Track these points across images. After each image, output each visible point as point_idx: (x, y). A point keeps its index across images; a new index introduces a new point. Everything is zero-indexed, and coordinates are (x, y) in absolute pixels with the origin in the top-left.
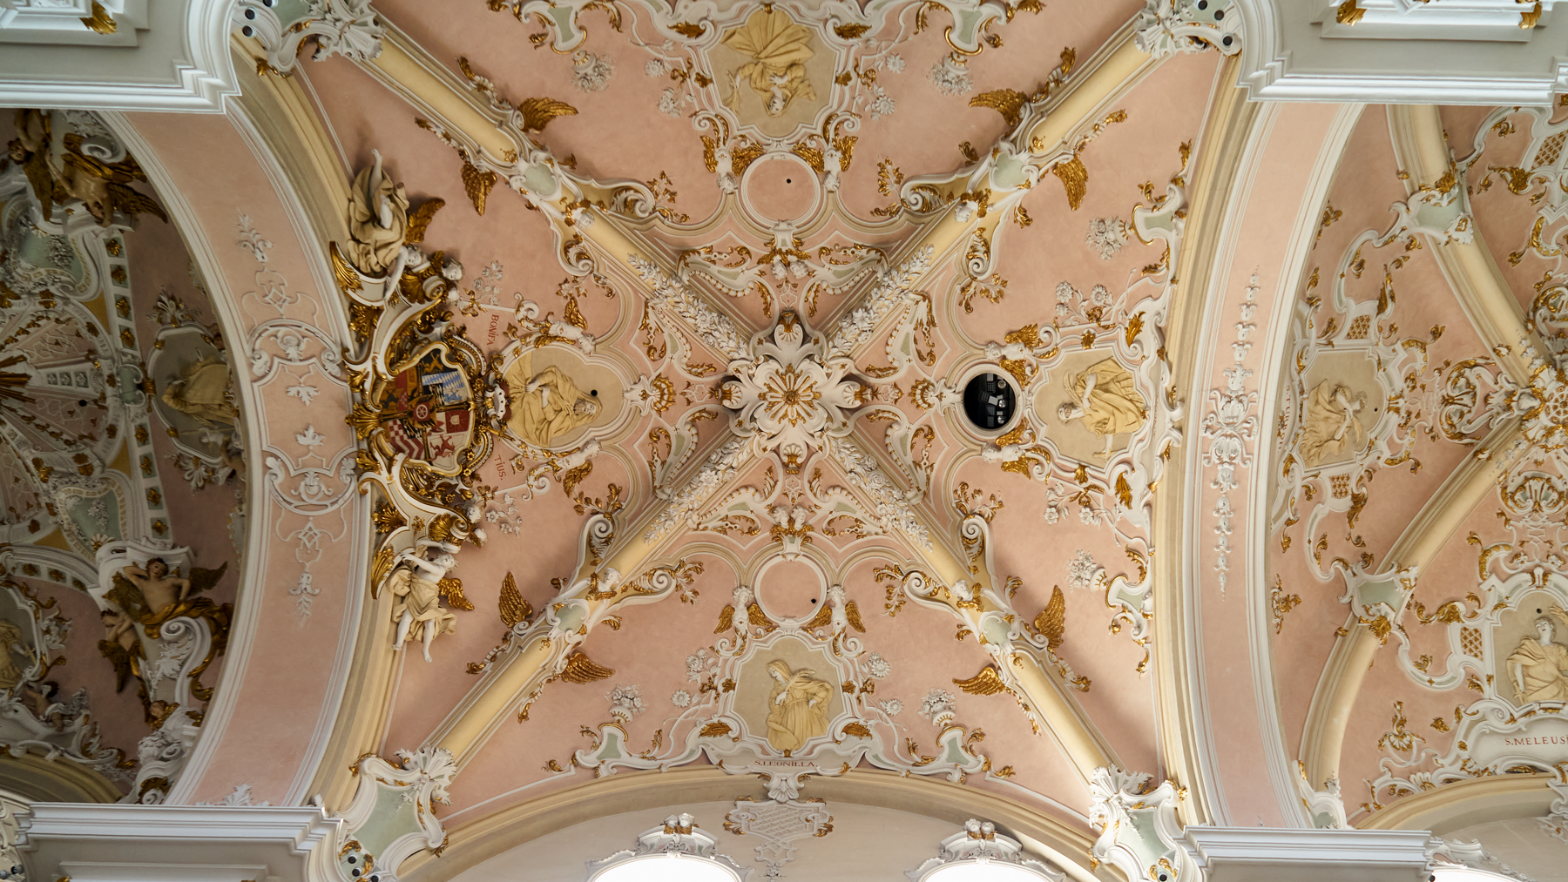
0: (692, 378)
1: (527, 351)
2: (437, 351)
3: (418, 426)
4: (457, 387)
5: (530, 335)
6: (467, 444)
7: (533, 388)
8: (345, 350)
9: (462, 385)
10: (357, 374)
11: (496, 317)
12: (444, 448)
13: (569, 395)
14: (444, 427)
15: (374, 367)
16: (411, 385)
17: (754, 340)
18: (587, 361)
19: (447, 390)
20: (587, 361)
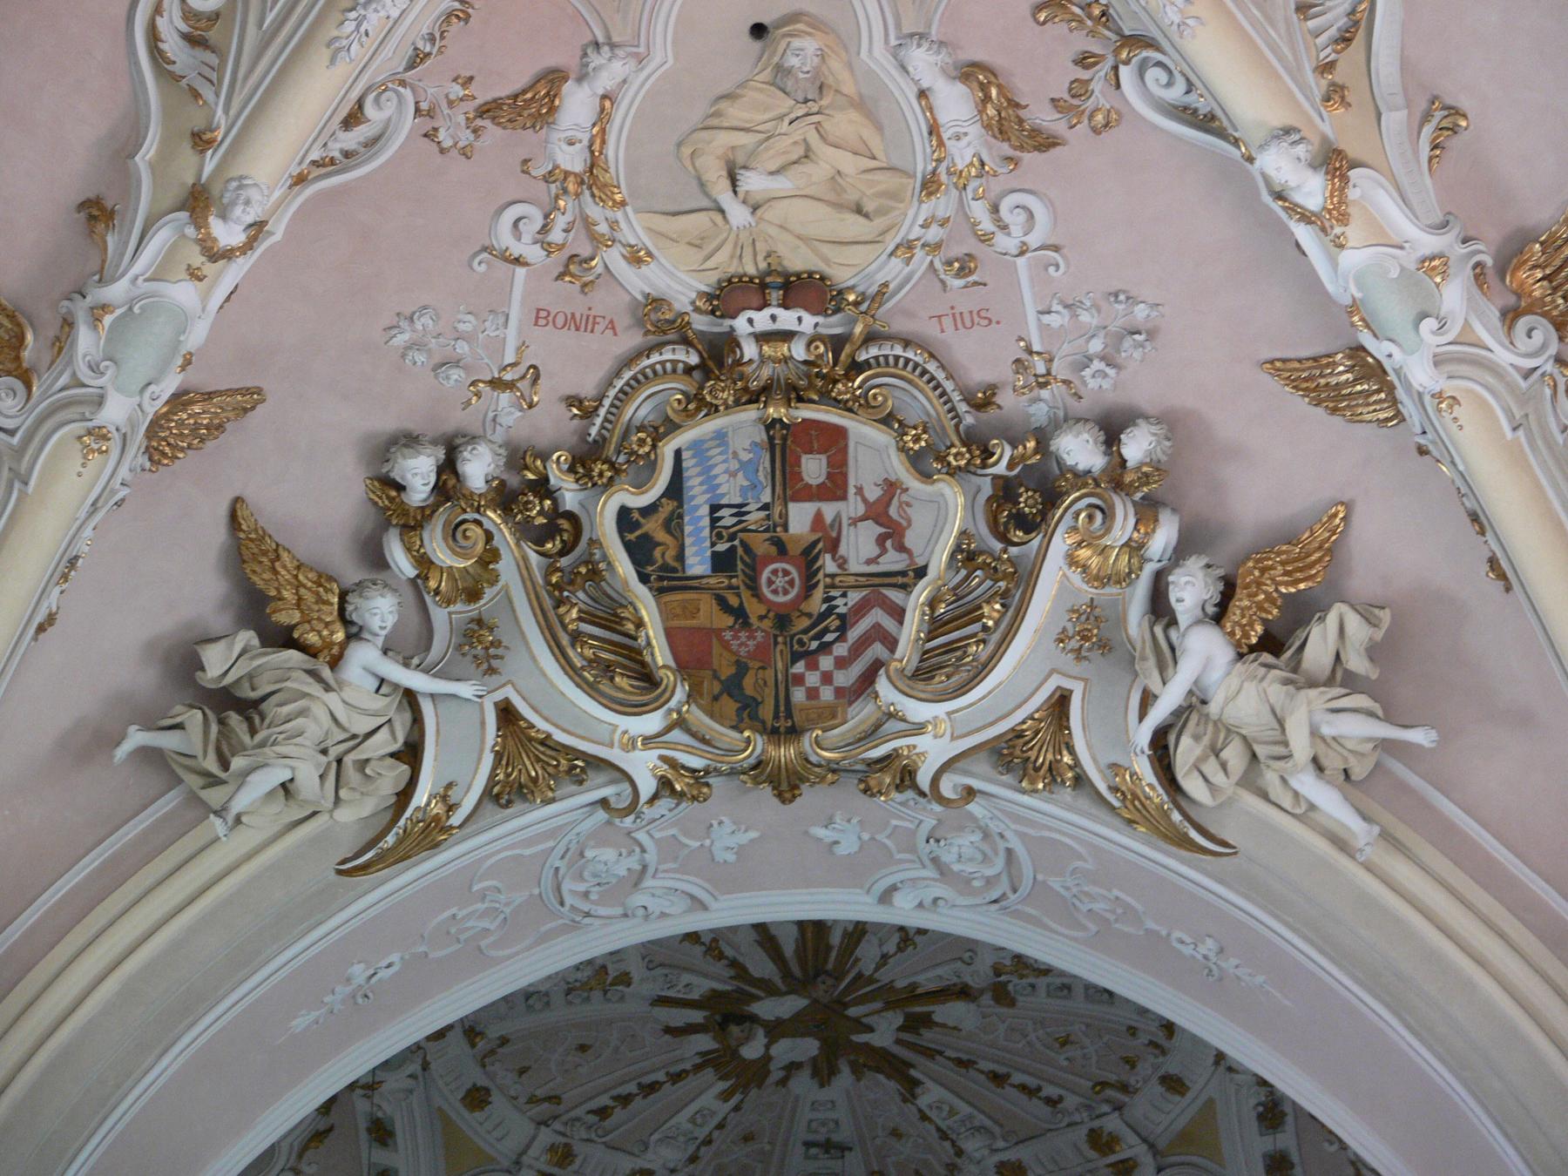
1: (634, 228)
2: (624, 513)
3: (816, 604)
4: (723, 451)
5: (588, 224)
7: (739, 215)
8: (604, 803)
9: (720, 437)
10: (665, 784)
11: (541, 317)
12: (886, 520)
13: (760, 106)
14: (829, 510)
15: (649, 741)
16: (709, 614)
18: (662, 55)
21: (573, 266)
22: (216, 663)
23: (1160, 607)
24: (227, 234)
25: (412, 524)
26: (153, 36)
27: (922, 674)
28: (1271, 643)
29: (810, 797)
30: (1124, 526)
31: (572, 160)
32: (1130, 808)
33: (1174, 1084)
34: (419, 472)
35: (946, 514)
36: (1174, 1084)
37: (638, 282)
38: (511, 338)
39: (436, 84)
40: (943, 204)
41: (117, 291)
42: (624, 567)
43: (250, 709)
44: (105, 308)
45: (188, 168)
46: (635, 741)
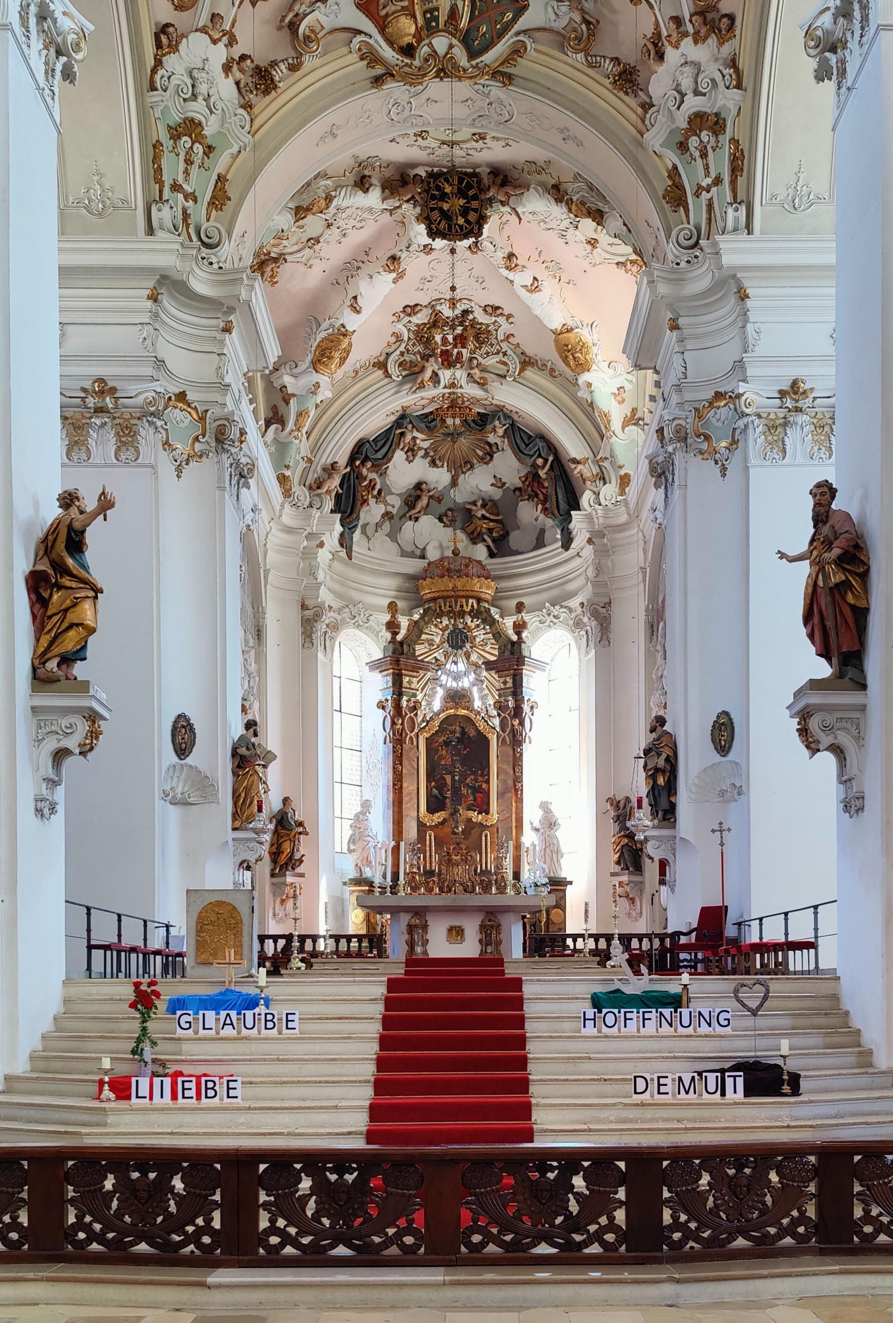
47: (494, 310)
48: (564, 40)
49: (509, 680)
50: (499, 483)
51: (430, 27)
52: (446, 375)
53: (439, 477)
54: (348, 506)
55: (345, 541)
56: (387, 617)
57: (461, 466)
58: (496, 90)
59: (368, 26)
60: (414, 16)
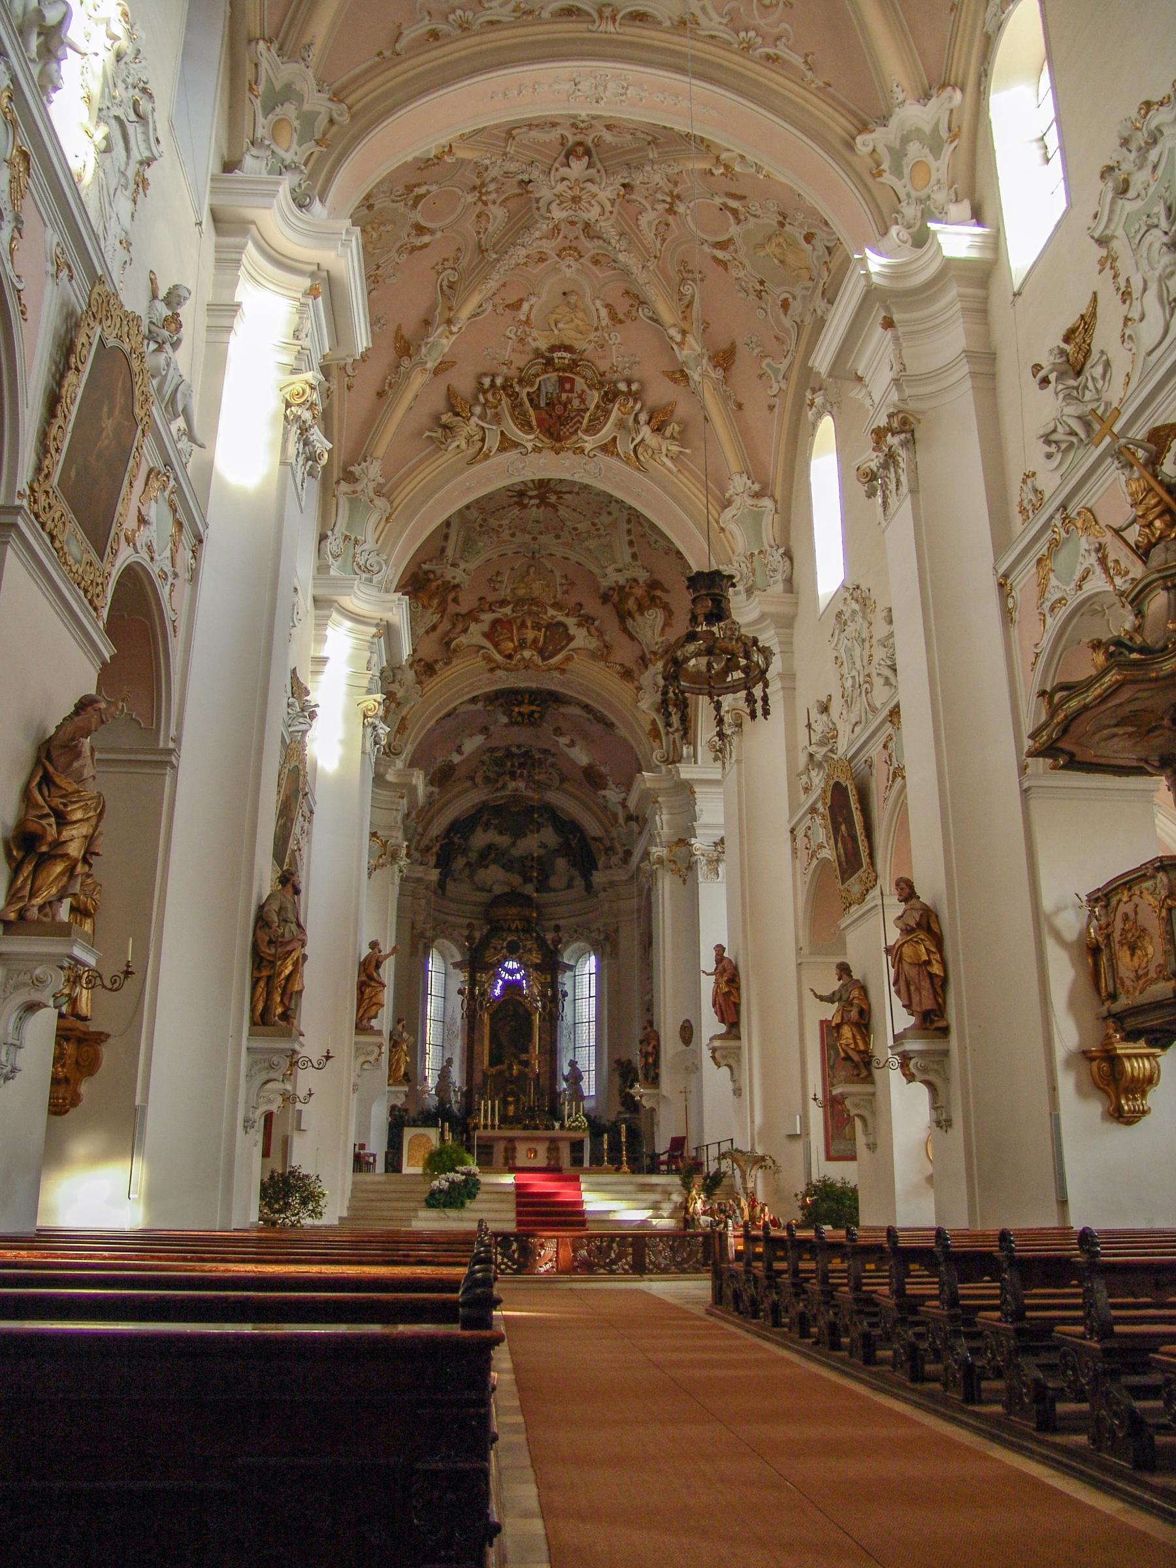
0: (561, 236)
2: (528, 394)
3: (566, 414)
6: (582, 381)
7: (556, 332)
10: (534, 450)
16: (544, 415)
17: (536, 214)
18: (544, 297)
19: (550, 390)
20: (544, 297)
21: (521, 340)
22: (446, 418)
23: (636, 421)
24: (455, 329)
25: (485, 392)
26: (441, 286)
27: (586, 431)
28: (658, 430)
29: (562, 454)
30: (631, 403)
31: (523, 318)
32: (627, 461)
33: (609, 513)
34: (487, 381)
35: (594, 398)
36: (609, 513)
37: (534, 345)
38: (507, 354)
39: (497, 300)
40: (598, 333)
41: (431, 340)
42: (528, 404)
43: (450, 429)
44: (427, 344)
45: (447, 315)
46: (528, 440)
47: (546, 751)
48: (593, 655)
49: (549, 977)
50: (543, 845)
51: (523, 645)
52: (512, 785)
53: (503, 841)
54: (444, 862)
55: (442, 885)
56: (466, 933)
57: (518, 833)
58: (556, 674)
59: (489, 645)
60: (512, 641)
